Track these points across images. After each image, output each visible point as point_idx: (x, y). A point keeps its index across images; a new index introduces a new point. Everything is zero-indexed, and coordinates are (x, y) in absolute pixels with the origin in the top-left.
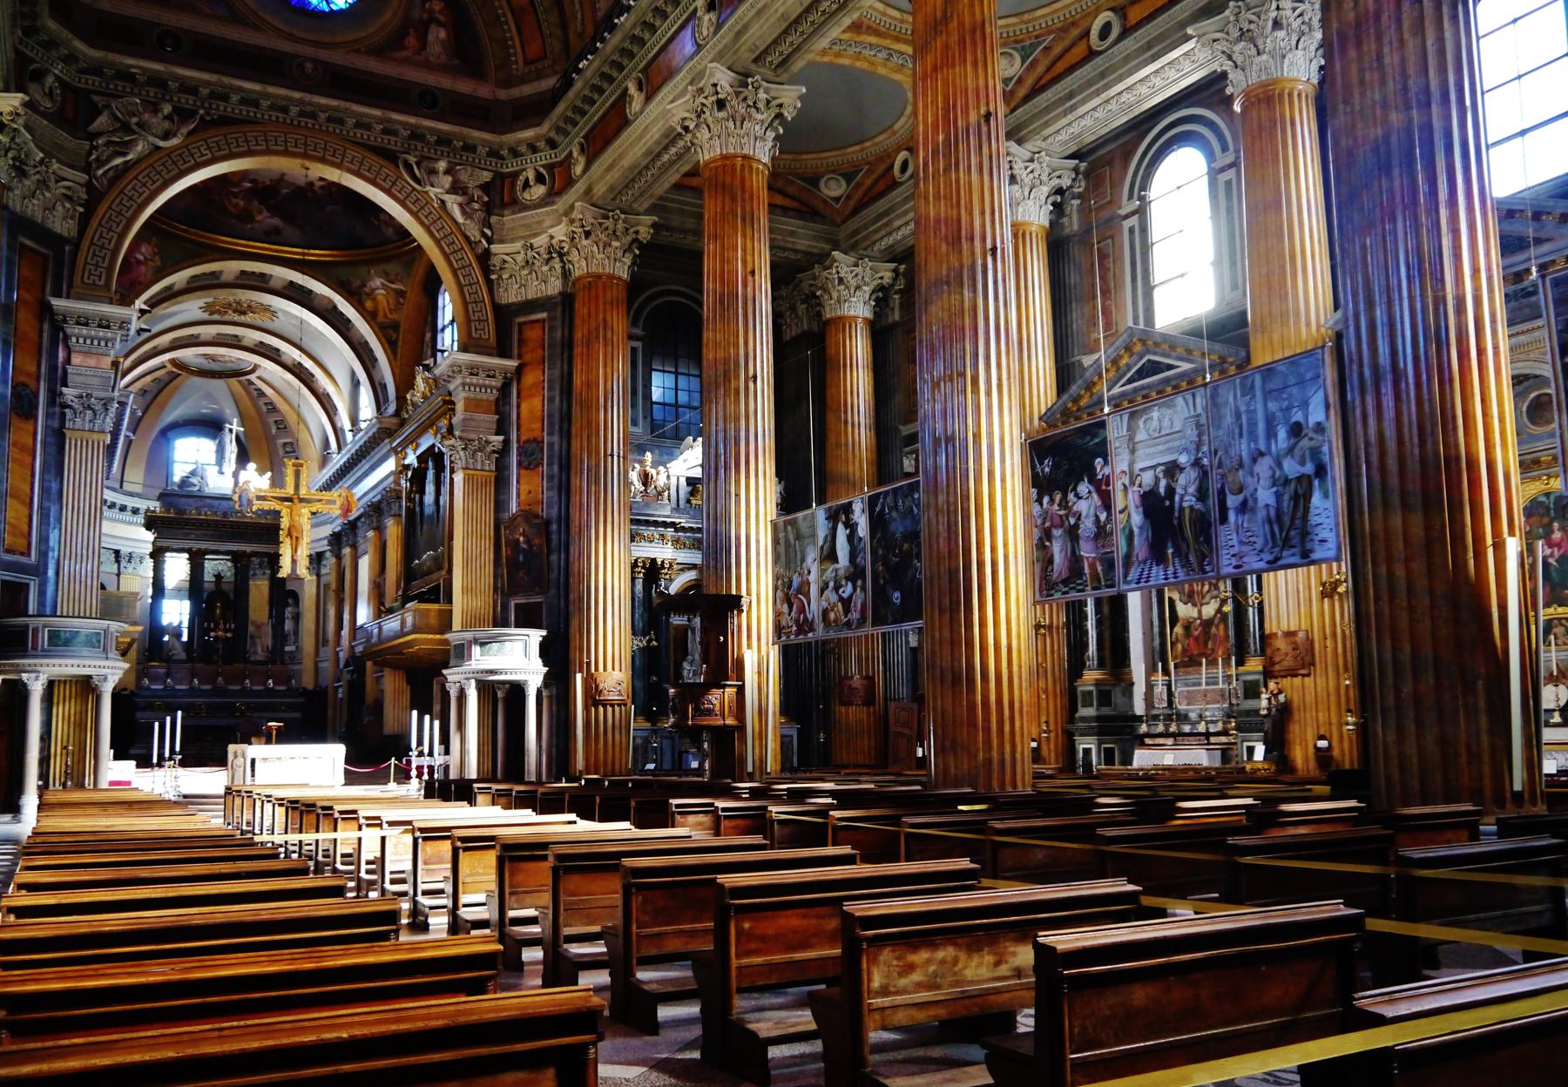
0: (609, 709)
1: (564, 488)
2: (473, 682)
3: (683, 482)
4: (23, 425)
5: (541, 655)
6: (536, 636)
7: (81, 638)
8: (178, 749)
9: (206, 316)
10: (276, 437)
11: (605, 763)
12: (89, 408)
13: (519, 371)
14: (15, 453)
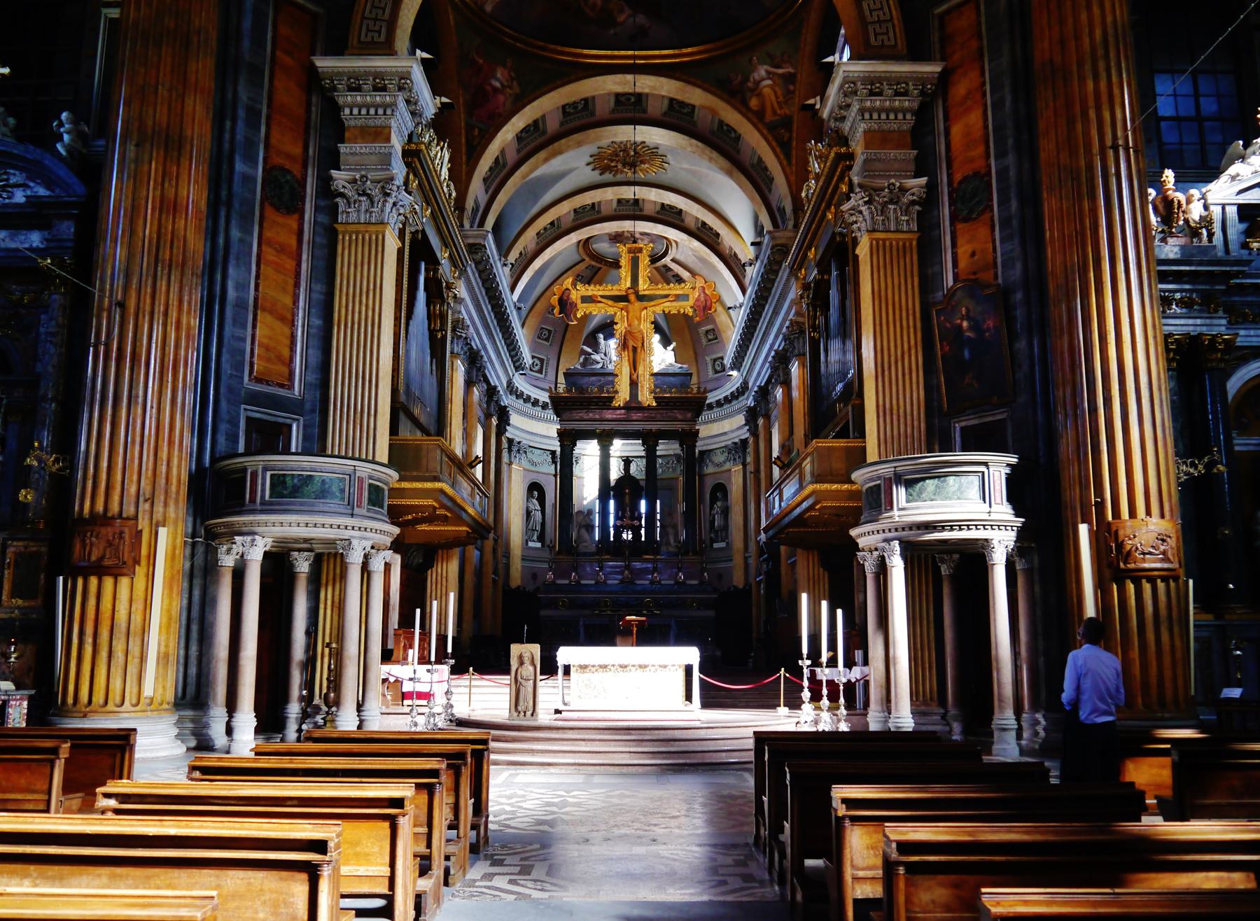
0: (1147, 587)
1: (1029, 232)
2: (896, 543)
3: (1232, 211)
4: (280, 220)
5: (1009, 500)
6: (999, 466)
7: (316, 486)
8: (450, 650)
9: (595, 177)
10: (700, 324)
11: (1145, 684)
12: (364, 194)
13: (944, 80)
14: (270, 254)
